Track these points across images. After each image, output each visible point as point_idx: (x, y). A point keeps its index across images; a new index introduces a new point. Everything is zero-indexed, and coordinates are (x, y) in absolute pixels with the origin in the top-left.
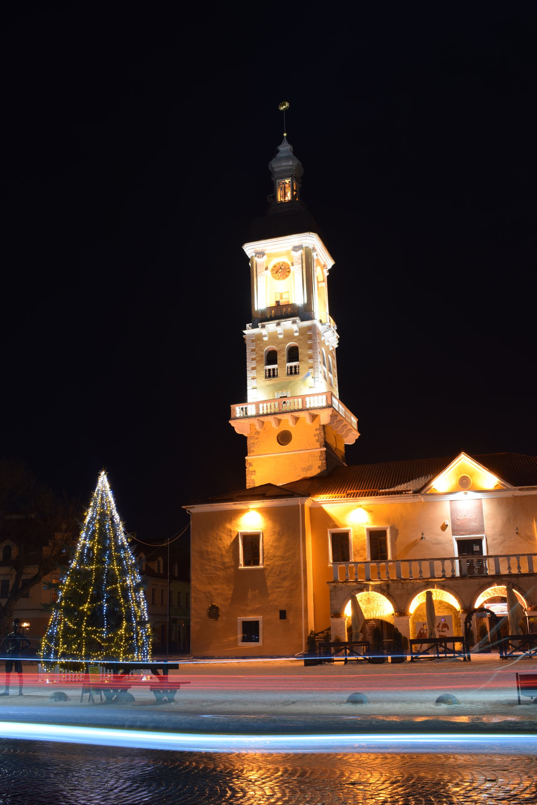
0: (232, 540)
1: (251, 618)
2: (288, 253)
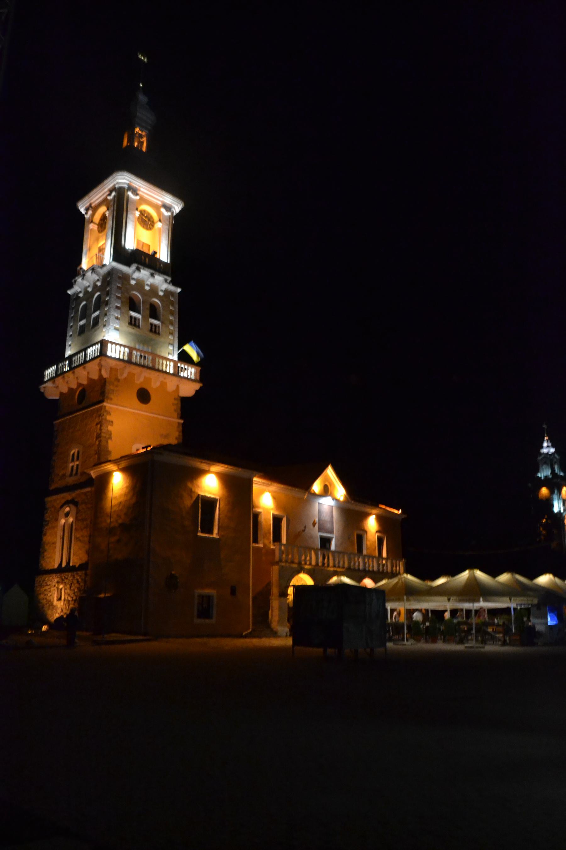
0: (192, 502)
1: (207, 591)
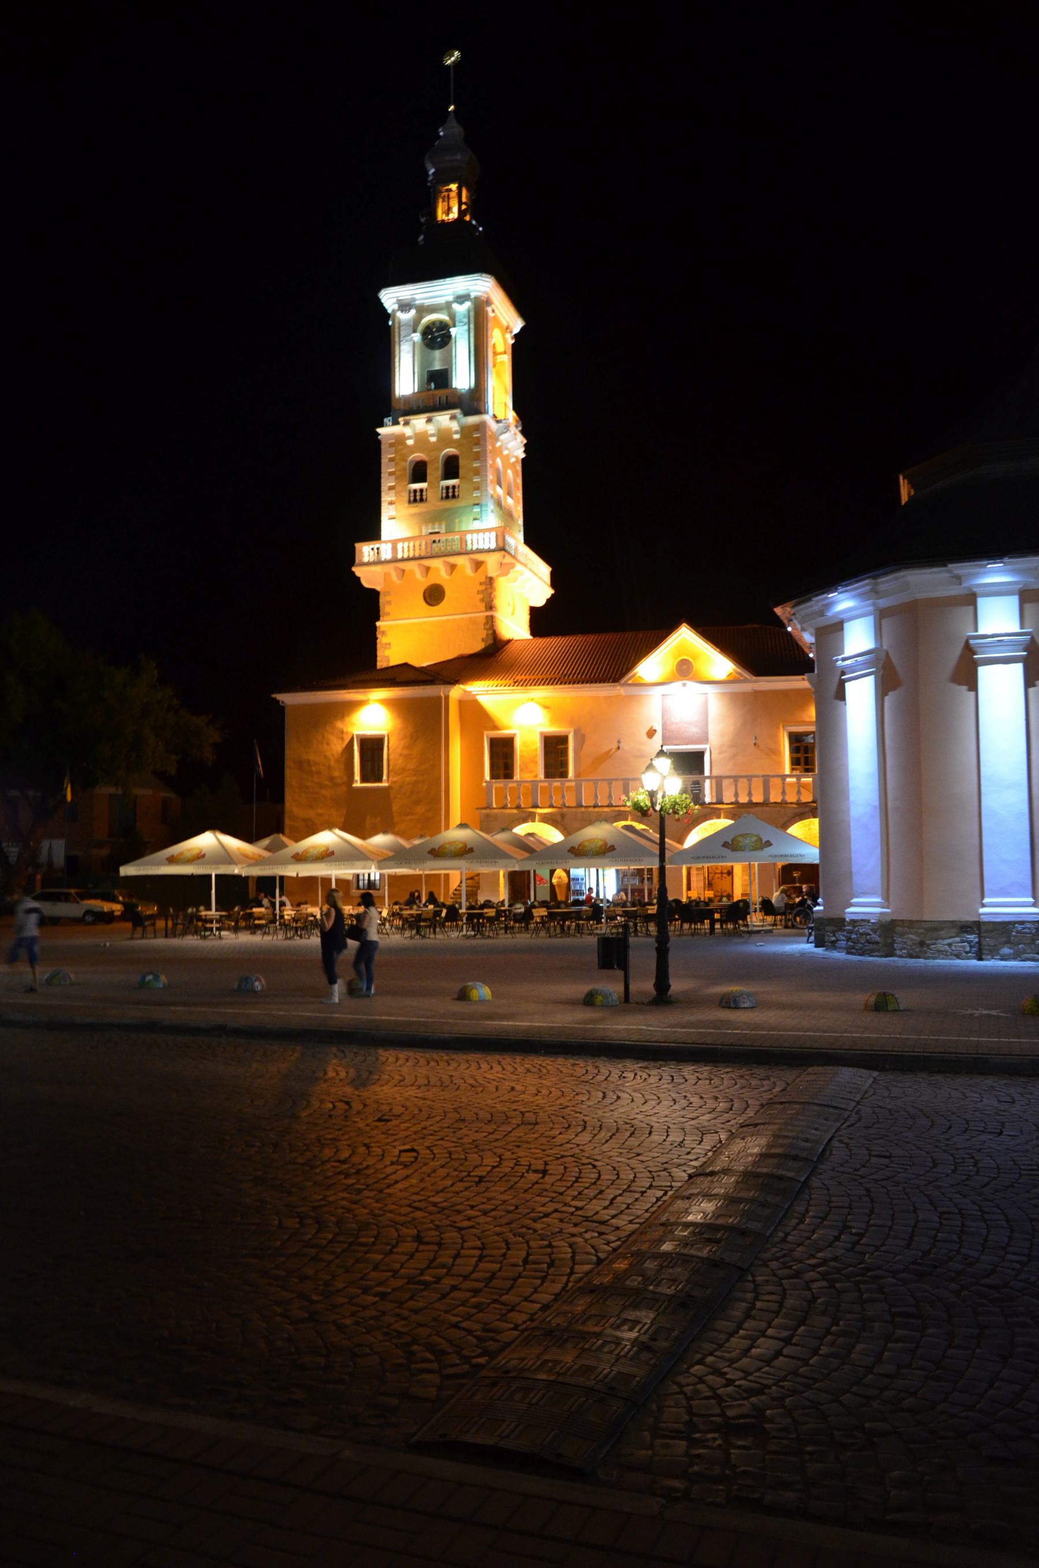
0: (344, 745)
2: (448, 306)
